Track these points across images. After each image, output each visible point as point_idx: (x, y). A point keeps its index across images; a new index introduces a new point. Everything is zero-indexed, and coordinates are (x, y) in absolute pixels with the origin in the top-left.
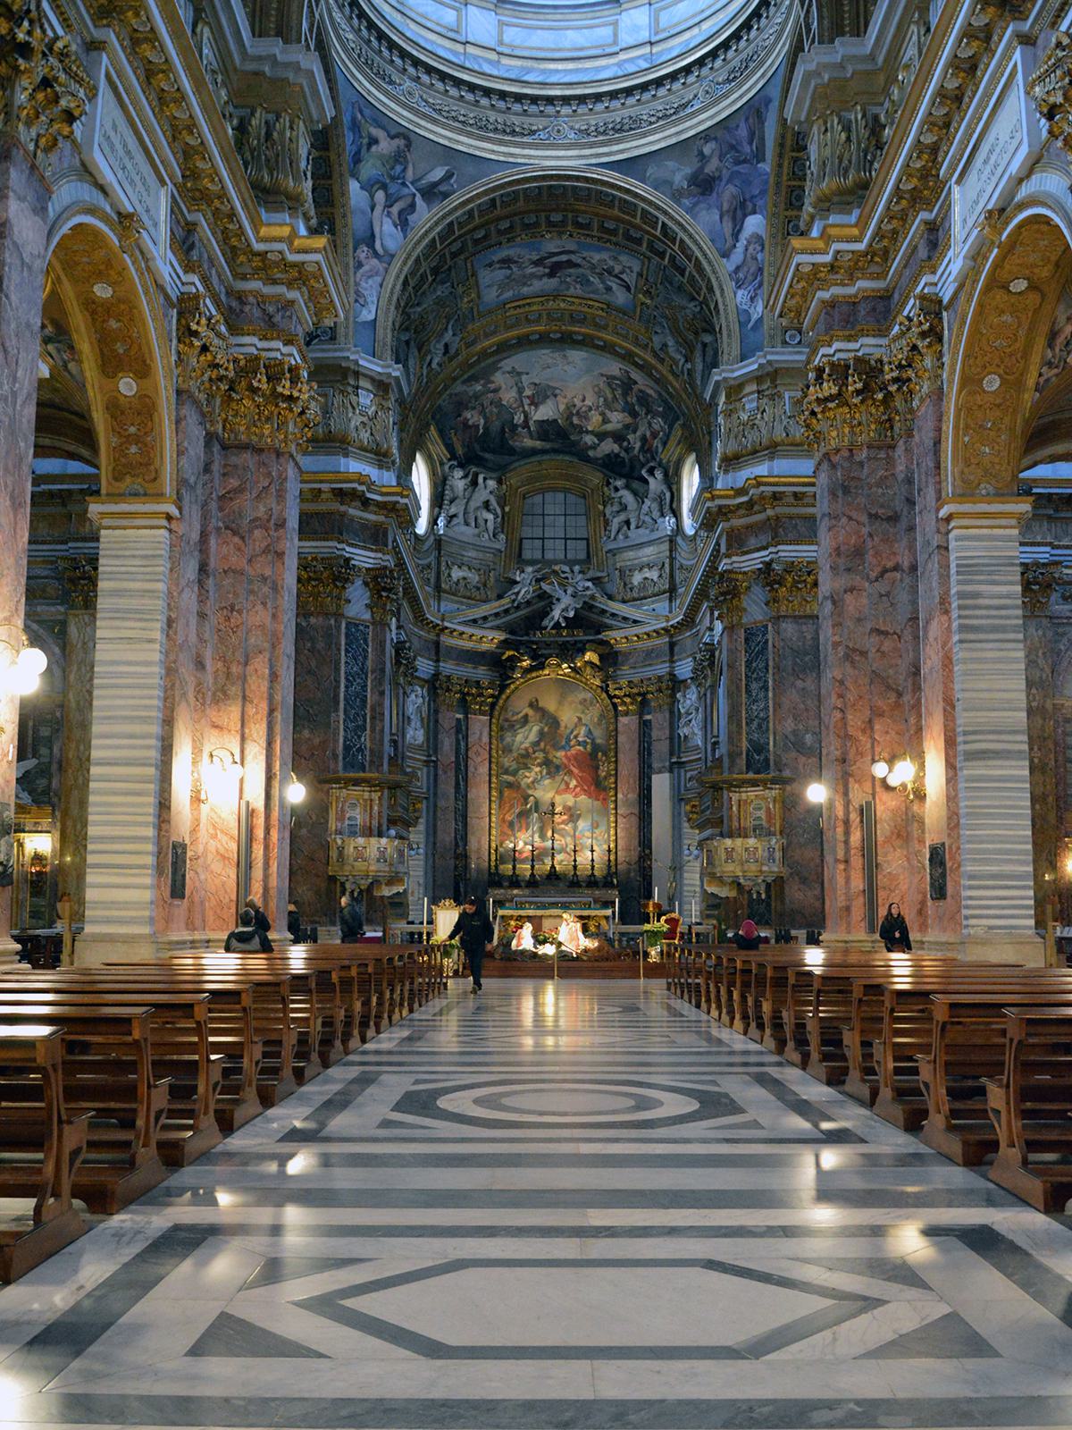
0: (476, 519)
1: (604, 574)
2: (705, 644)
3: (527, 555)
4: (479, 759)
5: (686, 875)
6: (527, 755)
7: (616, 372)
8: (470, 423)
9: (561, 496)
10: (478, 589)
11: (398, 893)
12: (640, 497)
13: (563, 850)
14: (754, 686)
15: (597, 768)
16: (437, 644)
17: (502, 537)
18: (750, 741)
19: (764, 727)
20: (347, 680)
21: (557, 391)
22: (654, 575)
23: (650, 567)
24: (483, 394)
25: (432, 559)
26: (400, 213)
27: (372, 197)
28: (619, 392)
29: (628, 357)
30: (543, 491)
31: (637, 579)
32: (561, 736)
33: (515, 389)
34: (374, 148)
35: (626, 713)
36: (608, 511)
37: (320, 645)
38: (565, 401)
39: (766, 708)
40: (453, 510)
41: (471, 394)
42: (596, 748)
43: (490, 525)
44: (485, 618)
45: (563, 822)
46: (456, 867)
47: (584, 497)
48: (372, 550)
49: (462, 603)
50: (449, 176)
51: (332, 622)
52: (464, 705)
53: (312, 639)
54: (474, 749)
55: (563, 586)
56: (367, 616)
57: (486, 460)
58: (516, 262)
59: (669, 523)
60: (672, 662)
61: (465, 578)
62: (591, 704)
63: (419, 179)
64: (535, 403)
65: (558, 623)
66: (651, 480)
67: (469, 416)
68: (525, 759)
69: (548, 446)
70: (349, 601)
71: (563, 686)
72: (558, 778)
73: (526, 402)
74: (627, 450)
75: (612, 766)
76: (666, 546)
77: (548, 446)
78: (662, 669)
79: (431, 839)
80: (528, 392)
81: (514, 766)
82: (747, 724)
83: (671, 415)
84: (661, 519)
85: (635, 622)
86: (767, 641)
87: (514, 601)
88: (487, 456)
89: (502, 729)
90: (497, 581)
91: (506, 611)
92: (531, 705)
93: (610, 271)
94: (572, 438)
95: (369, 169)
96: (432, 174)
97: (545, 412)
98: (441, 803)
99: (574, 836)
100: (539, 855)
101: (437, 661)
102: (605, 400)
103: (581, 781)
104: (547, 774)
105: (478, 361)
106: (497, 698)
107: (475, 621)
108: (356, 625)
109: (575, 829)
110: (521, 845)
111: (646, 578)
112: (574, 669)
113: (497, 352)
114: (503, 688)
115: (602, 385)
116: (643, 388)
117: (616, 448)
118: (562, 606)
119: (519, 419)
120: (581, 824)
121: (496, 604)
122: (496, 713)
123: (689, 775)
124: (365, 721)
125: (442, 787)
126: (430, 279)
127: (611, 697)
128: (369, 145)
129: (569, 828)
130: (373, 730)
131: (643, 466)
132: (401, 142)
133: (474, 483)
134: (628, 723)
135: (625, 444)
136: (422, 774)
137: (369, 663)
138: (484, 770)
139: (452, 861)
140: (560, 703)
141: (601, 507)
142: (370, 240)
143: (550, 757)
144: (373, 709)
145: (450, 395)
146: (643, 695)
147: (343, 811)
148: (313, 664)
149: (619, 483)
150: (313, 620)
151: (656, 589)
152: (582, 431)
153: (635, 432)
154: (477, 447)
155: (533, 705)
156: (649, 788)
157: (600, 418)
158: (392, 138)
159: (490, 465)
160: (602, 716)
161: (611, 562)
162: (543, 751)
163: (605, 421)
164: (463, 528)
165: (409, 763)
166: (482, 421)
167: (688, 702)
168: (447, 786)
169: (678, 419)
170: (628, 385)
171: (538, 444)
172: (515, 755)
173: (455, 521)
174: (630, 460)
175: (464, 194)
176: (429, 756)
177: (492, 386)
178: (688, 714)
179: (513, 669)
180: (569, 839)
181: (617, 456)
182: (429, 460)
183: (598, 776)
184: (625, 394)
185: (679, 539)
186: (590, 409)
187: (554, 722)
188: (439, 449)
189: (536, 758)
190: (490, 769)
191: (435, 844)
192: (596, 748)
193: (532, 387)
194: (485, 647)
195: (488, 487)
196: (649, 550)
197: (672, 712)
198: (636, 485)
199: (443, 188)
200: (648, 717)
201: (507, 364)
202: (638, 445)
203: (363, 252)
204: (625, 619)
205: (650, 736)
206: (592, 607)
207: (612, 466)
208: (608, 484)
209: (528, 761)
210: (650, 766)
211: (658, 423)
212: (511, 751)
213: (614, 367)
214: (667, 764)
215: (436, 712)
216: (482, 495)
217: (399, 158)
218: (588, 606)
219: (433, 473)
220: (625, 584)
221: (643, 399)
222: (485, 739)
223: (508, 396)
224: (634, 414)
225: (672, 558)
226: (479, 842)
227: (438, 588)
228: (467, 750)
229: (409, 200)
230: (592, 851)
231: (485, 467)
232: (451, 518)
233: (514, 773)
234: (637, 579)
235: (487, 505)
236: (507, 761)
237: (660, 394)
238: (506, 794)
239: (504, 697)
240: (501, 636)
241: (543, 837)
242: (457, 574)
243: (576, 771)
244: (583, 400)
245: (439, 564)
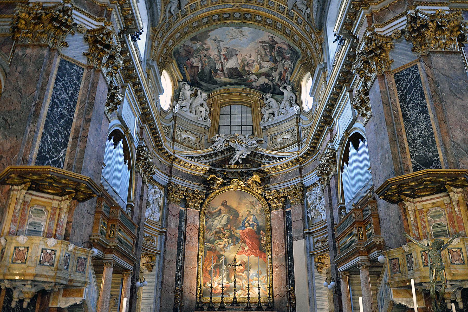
0: (196, 111)
1: (262, 139)
2: (329, 148)
4: (193, 233)
5: (318, 302)
6: (220, 232)
7: (267, 39)
8: (194, 65)
9: (238, 107)
10: (195, 143)
11: (76, 305)
13: (241, 288)
14: (412, 113)
15: (260, 239)
16: (171, 167)
18: (416, 158)
19: (429, 143)
20: (53, 101)
21: (238, 53)
23: (286, 132)
24: (200, 50)
28: (268, 50)
29: (274, 25)
31: (279, 140)
32: (240, 222)
33: (217, 50)
35: (276, 208)
36: (263, 110)
37: (30, 69)
38: (242, 58)
39: (429, 127)
40: (184, 103)
41: (195, 48)
42: (259, 228)
43: (203, 114)
44: (198, 157)
45: (241, 271)
46: (175, 299)
47: (251, 107)
48: (95, 19)
49: (186, 149)
51: (46, 52)
52: (185, 201)
53: (25, 65)
54: (190, 227)
56: (84, 61)
57: (202, 85)
59: (296, 108)
60: (302, 177)
61: (189, 138)
62: (256, 204)
65: (237, 163)
66: (285, 91)
67: (194, 61)
68: (219, 234)
69: (233, 81)
70: (66, 45)
71: (240, 193)
72: (238, 245)
73: (223, 57)
74: (272, 81)
75: (269, 237)
77: (233, 81)
78: (296, 181)
79: (160, 279)
80: (223, 52)
81: (213, 238)
82: (410, 144)
83: (295, 55)
84: (292, 108)
85: (280, 158)
86: (418, 77)
87: (214, 150)
88: (203, 83)
89: (206, 217)
91: (210, 156)
92: (223, 204)
94: (245, 77)
97: (231, 64)
98: (168, 257)
99: (248, 280)
100: (226, 291)
101: (170, 176)
102: (261, 56)
104: (231, 243)
105: (198, 26)
106: (204, 200)
107: (192, 158)
108: (73, 65)
109: (248, 275)
110: (215, 285)
111: (284, 138)
112: (247, 185)
113: (208, 23)
114: (207, 195)
115: (260, 48)
116: (279, 45)
117: (266, 81)
118: (240, 152)
119: (219, 66)
120: (252, 272)
121: (205, 151)
122: (203, 208)
123: (316, 239)
124: (67, 139)
125: (168, 247)
127: (267, 200)
129: (244, 274)
130: (74, 147)
131: (280, 86)
133: (196, 95)
134: (277, 213)
135: (271, 78)
136: (158, 239)
137: (79, 95)
138: (195, 239)
139: (173, 295)
140: (239, 204)
141: (260, 109)
143: (233, 233)
144: (77, 131)
145: (184, 45)
146: (286, 197)
147: (23, 215)
148: (20, 83)
149: (268, 95)
150: (28, 51)
151: (290, 142)
152: (249, 73)
153: (276, 71)
154: (198, 78)
156: (291, 250)
157: (259, 66)
159: (204, 88)
160: (262, 210)
161: (265, 133)
162: (230, 229)
163: (261, 67)
164: (189, 114)
165: (150, 231)
166: (200, 65)
167: (313, 197)
168: (172, 248)
169: (299, 57)
170: (272, 45)
171: (228, 80)
172: (214, 232)
173: (184, 109)
174: (274, 85)
176: (162, 228)
177: (205, 47)
178: (312, 203)
179: (213, 184)
180: (244, 281)
181: (267, 84)
182: (172, 76)
183: (261, 244)
184: (271, 52)
185: (302, 116)
186: (254, 62)
187: (236, 214)
188: (178, 74)
189: (225, 234)
190: (199, 239)
191: (162, 282)
192: (259, 228)
193: (225, 49)
194: (198, 173)
197: (303, 205)
198: (277, 96)
200: (289, 210)
201: (213, 34)
202: (278, 77)
205: (290, 220)
206: (256, 154)
207: (264, 89)
208: (263, 98)
209: (221, 235)
210: (291, 237)
211: (288, 63)
212: (211, 230)
213: (265, 36)
214: (302, 234)
215: (168, 204)
218: (254, 154)
219: (174, 84)
220: (273, 143)
221: (280, 53)
222: (197, 222)
223: (213, 53)
224: (275, 61)
225: (298, 127)
226: (191, 283)
227: (173, 140)
228: (186, 227)
230: (259, 288)
231: (201, 89)
233: (213, 242)
234: (279, 140)
235: (202, 105)
236: (209, 235)
237: (289, 46)
238: (208, 254)
239: (208, 199)
240: (208, 168)
241: (229, 280)
242: (184, 136)
243: (248, 241)
244: (250, 57)
245: (174, 127)
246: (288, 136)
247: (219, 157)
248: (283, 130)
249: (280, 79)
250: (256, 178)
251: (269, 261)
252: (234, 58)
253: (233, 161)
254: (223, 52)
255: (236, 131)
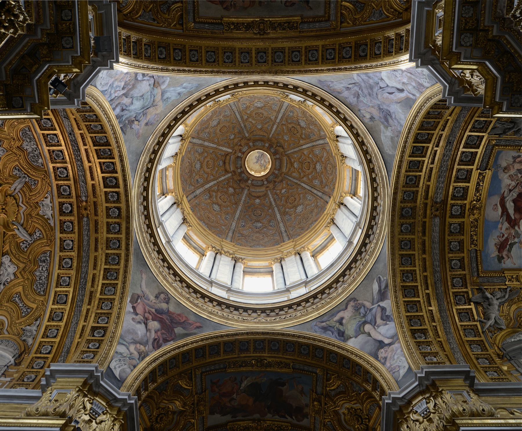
26: (382, 319)
27: (364, 333)
34: (344, 321)
58: (507, 240)
63: (373, 299)
95: (350, 328)
96: (374, 291)
126: (472, 306)
128: (341, 323)
132: (352, 303)
142: (381, 344)
158: (346, 308)
199: (383, 287)
203: (382, 353)
217: (357, 309)
229: (379, 310)
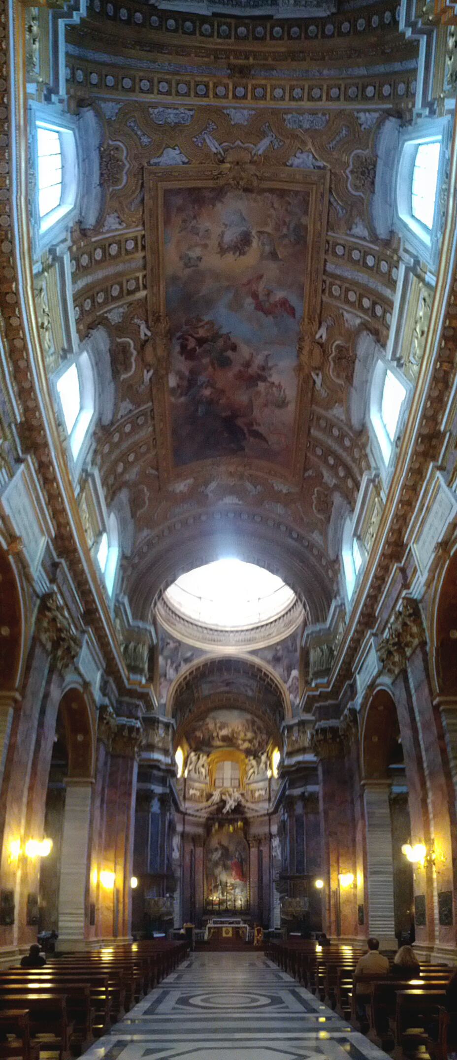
3: (217, 784)
12: (259, 763)
17: (208, 778)
22: (263, 792)
23: (261, 789)
25: (182, 786)
28: (250, 726)
30: (224, 761)
31: (257, 794)
40: (191, 768)
50: (192, 655)
55: (230, 796)
64: (221, 728)
65: (228, 812)
68: (216, 864)
76: (267, 783)
83: (269, 734)
90: (206, 794)
91: (209, 807)
93: (247, 685)
97: (224, 732)
103: (237, 874)
107: (198, 811)
117: (250, 745)
119: (215, 734)
120: (237, 890)
129: (232, 892)
133: (199, 758)
149: (252, 758)
155: (220, 843)
163: (245, 735)
175: (197, 661)
188: (186, 747)
192: (242, 860)
195: (203, 759)
196: (261, 785)
201: (212, 715)
202: (257, 745)
204: (253, 810)
211: (264, 737)
213: (249, 717)
216: (201, 762)
221: (259, 728)
223: (211, 726)
224: (255, 733)
232: (189, 771)
234: (257, 794)
235: (203, 766)
246: (263, 792)
247: (215, 807)
248: (260, 787)
249: (259, 745)
250: (240, 824)
251: (248, 883)
252: (226, 729)
253: (225, 811)
254: (218, 725)
255: (227, 784)
